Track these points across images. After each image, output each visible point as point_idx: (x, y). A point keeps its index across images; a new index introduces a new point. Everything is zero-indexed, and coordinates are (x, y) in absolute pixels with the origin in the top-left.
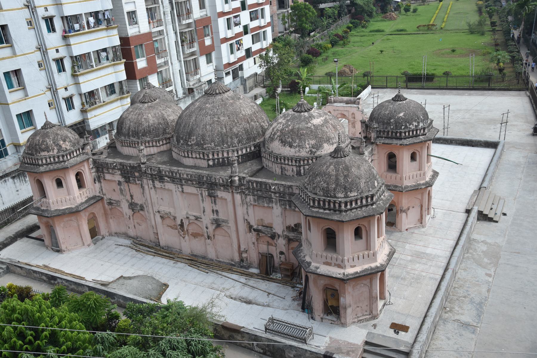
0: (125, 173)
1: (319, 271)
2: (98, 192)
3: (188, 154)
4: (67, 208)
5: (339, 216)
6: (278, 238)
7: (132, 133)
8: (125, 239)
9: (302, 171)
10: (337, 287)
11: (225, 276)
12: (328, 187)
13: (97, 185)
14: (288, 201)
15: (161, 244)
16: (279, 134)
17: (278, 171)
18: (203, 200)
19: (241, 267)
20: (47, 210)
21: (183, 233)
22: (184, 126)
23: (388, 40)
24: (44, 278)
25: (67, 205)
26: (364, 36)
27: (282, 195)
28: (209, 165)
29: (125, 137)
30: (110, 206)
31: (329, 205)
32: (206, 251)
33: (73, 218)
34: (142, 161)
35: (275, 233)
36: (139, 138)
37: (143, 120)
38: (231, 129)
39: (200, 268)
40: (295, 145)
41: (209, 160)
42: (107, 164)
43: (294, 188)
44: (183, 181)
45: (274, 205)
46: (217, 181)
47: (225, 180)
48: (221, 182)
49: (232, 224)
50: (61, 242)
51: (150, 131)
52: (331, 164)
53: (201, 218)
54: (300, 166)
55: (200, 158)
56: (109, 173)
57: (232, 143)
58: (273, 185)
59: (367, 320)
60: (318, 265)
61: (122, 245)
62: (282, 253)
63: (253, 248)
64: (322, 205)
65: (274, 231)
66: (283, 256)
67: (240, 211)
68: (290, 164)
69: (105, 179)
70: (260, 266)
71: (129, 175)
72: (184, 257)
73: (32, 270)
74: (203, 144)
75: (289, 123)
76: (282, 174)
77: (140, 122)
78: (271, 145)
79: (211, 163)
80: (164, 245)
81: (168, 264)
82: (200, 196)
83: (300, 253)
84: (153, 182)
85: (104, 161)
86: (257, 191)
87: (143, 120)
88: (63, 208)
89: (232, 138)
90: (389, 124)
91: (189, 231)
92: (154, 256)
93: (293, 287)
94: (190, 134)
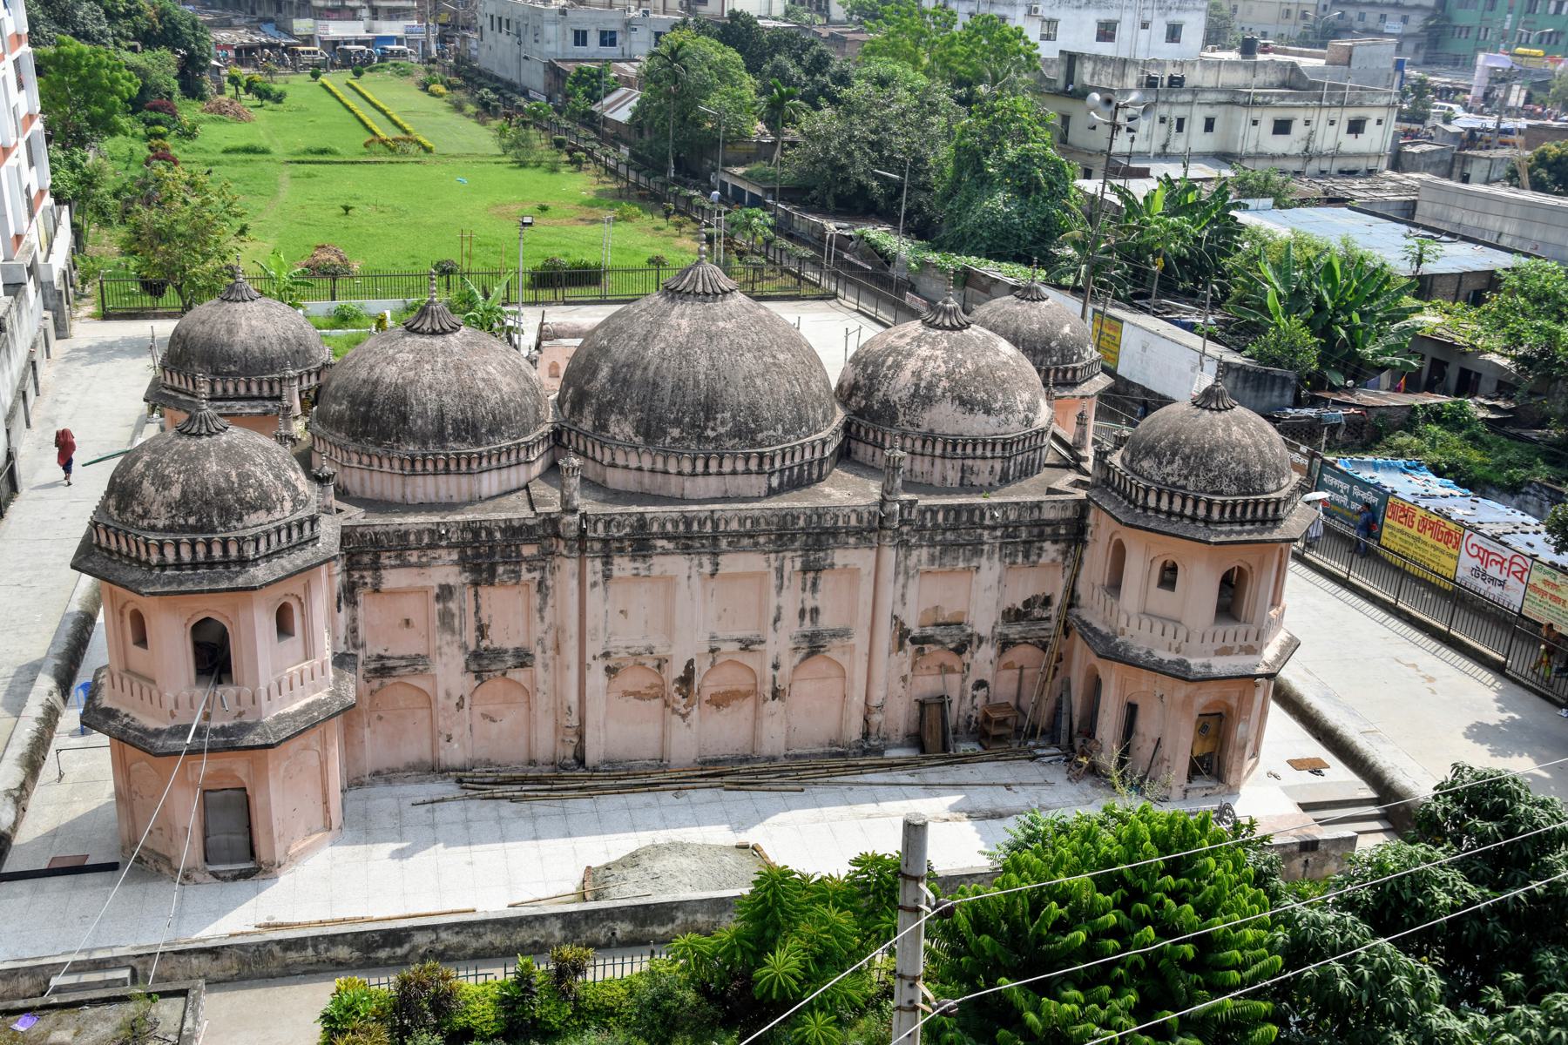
1: (1215, 671)
2: (342, 639)
3: (707, 466)
4: (309, 707)
7: (456, 428)
8: (422, 782)
10: (1233, 702)
11: (857, 784)
13: (343, 617)
14: (1025, 542)
15: (593, 755)
16: (944, 383)
17: (953, 477)
18: (780, 588)
19: (865, 753)
20: (244, 728)
21: (684, 701)
22: (677, 387)
23: (309, 176)
24: (342, 952)
25: (304, 695)
26: (218, 163)
27: (1009, 530)
29: (425, 444)
30: (376, 683)
32: (755, 737)
33: (313, 737)
35: (971, 635)
36: (478, 444)
40: (997, 405)
41: (771, 474)
42: (407, 533)
43: (1046, 507)
44: (724, 543)
45: (984, 561)
46: (840, 523)
47: (866, 515)
48: (853, 522)
49: (860, 640)
50: (276, 835)
52: (1227, 422)
53: (762, 642)
55: (748, 472)
56: (405, 564)
57: (815, 420)
58: (991, 507)
61: (443, 800)
62: (981, 684)
63: (900, 691)
65: (969, 630)
66: (982, 693)
68: (989, 454)
69: (377, 591)
70: (917, 740)
73: (279, 942)
74: (754, 432)
76: (961, 484)
77: (475, 391)
78: (927, 415)
79: (775, 482)
81: (663, 802)
83: (1126, 650)
84: (607, 562)
85: (391, 529)
86: (945, 531)
88: (296, 707)
90: (1047, 351)
92: (591, 796)
93: (1032, 759)
94: (710, 407)
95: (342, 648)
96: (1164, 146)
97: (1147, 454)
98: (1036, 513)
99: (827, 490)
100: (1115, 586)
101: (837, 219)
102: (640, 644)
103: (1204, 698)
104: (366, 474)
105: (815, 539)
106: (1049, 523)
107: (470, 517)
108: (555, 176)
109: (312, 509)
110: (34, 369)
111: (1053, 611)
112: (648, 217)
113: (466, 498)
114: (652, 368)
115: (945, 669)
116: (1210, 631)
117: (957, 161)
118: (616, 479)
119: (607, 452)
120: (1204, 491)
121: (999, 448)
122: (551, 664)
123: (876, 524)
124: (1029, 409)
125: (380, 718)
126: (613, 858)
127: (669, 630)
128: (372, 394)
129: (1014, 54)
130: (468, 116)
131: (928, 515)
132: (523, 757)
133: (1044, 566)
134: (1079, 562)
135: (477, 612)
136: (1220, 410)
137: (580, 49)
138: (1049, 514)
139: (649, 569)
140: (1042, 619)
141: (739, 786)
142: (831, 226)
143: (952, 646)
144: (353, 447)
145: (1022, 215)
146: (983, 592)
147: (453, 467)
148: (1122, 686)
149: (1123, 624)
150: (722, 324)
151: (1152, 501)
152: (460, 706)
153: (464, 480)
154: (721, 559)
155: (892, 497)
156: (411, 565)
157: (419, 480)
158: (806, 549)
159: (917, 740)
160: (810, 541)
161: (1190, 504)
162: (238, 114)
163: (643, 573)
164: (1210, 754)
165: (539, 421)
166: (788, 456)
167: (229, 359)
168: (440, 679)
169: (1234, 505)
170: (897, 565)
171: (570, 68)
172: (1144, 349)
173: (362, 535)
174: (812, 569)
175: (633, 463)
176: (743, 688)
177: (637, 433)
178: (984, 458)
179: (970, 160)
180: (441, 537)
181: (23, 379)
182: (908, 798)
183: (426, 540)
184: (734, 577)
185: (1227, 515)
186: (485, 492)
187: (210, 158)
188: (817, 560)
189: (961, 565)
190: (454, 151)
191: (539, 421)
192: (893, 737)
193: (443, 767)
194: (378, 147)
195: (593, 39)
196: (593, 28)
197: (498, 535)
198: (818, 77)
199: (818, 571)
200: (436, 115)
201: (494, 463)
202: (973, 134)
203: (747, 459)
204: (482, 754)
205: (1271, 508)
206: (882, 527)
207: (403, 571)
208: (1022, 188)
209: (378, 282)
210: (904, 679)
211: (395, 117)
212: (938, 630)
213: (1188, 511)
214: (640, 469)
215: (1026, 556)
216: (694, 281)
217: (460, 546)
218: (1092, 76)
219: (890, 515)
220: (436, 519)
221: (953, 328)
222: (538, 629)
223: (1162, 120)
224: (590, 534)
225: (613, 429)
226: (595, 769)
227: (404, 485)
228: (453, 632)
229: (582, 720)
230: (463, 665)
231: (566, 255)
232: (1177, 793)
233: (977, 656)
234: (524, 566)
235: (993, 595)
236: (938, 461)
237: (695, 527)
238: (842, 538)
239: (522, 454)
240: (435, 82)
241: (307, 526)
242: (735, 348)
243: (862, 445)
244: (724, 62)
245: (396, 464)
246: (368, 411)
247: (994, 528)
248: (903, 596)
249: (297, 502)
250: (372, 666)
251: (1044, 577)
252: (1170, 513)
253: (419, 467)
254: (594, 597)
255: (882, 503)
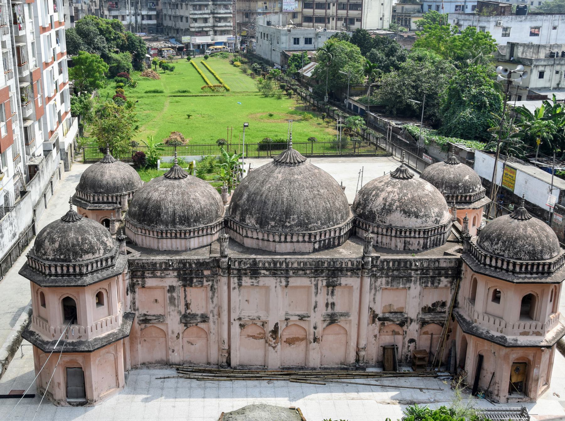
0: (185, 274)
1: (519, 343)
3: (286, 238)
5: (550, 278)
6: (410, 324)
9: (428, 244)
10: (531, 358)
11: (351, 383)
12: (534, 250)
13: (129, 297)
14: (431, 277)
15: (234, 363)
16: (397, 204)
17: (400, 246)
18: (317, 293)
19: (357, 369)
21: (274, 341)
22: (274, 204)
23: (177, 102)
26: (142, 97)
28: (314, 248)
29: (167, 225)
31: (538, 268)
34: (226, 253)
35: (407, 318)
36: (189, 226)
37: (192, 201)
38: (334, 203)
39: (308, 382)
40: (421, 214)
41: (315, 243)
42: (156, 263)
44: (291, 273)
45: (412, 285)
46: (344, 266)
47: (355, 263)
48: (350, 265)
49: (354, 317)
51: (203, 215)
52: (525, 226)
53: (309, 317)
54: (427, 238)
55: (304, 241)
56: (155, 277)
57: (337, 219)
58: (415, 260)
59: (545, 390)
60: (514, 337)
62: (412, 341)
64: (529, 270)
65: (406, 316)
66: (412, 345)
67: (367, 298)
68: (417, 236)
69: (143, 287)
70: (381, 364)
71: (193, 275)
72: (276, 373)
74: (307, 224)
75: (405, 191)
76: (404, 249)
77: (189, 204)
78: (388, 218)
79: (317, 246)
80: (238, 363)
81: (262, 385)
82: (314, 287)
83: (477, 330)
84: (240, 279)
85: (149, 261)
86: (393, 270)
87: (192, 201)
89: (336, 214)
90: (457, 188)
91: (282, 337)
92: (231, 380)
93: (435, 377)
94: (288, 213)
95: (129, 310)
96: (558, 84)
97: (487, 239)
98: (437, 264)
99: (341, 250)
100: (473, 300)
101: (397, 120)
102: (254, 315)
103: (515, 355)
104: (144, 237)
105: (332, 273)
106: (443, 269)
107: (182, 258)
108: (280, 101)
109: (112, 253)
110: (52, 184)
111: (447, 309)
112: (316, 119)
113: (184, 249)
114: (264, 195)
115: (395, 333)
116: (517, 324)
117: (450, 95)
118: (248, 242)
119: (244, 231)
120: (512, 258)
121: (422, 233)
122: (216, 322)
123: (360, 266)
124: (438, 216)
125: (145, 340)
126: (235, 409)
127: (267, 310)
128: (147, 204)
129: (483, 45)
130: (248, 75)
131: (385, 263)
132: (205, 361)
133: (441, 288)
134: (458, 287)
135: (185, 298)
136: (522, 220)
137: (296, 46)
138: (443, 265)
139: (258, 282)
140: (441, 312)
141: (297, 380)
142: (393, 123)
143: (398, 322)
144: (139, 226)
145: (478, 118)
146: (413, 299)
147: (178, 235)
148: (476, 346)
149: (476, 317)
150: (296, 176)
151: (488, 262)
152: (178, 337)
153: (183, 241)
154: (290, 279)
155: (368, 255)
156: (157, 277)
157: (165, 240)
158: (328, 277)
159: (381, 364)
160: (330, 273)
161: (505, 263)
162: (154, 77)
163: (255, 284)
164: (521, 382)
165: (217, 216)
166: (323, 235)
167: (101, 187)
168: (169, 325)
169: (527, 265)
170: (371, 285)
171: (290, 54)
172: (526, 182)
173: (137, 263)
174: (332, 286)
175: (255, 236)
176: (301, 337)
177: (257, 223)
178: (415, 238)
179: (455, 94)
180: (170, 266)
181: (46, 189)
182: (373, 391)
183: (164, 267)
184: (296, 287)
185: (523, 269)
186: (192, 246)
187: (139, 95)
188: (333, 282)
189: (401, 286)
190: (238, 90)
191: (217, 216)
192: (371, 363)
193: (171, 363)
194: (207, 89)
195: (302, 41)
196: (302, 37)
197: (194, 266)
198: (391, 58)
199: (334, 286)
200: (234, 75)
201: (196, 234)
202: (457, 83)
203: (304, 236)
204: (187, 358)
205: (546, 267)
206: (363, 268)
207: (154, 279)
208: (478, 106)
209: (194, 148)
210: (375, 336)
211: (217, 76)
212: (391, 315)
213: (505, 267)
214: (258, 239)
215: (433, 283)
216: (286, 158)
217: (178, 270)
218: (523, 53)
219: (367, 263)
220: (168, 258)
221: (404, 178)
222: (211, 306)
223: (557, 72)
224: (232, 267)
225: (247, 221)
226: (235, 368)
227: (158, 243)
228: (175, 306)
229: (229, 346)
230: (179, 320)
231: (276, 136)
232: (503, 399)
233: (410, 328)
234: (205, 279)
235: (417, 300)
236: (393, 239)
237: (278, 265)
238: (345, 272)
239: (209, 231)
240: (236, 61)
241: (109, 260)
242: (301, 187)
243: (360, 230)
244: (352, 52)
245: (155, 234)
246: (145, 211)
247: (417, 270)
248: (374, 299)
249: (105, 249)
250: (141, 318)
251: (441, 293)
252: (496, 267)
253: (164, 235)
254: (235, 294)
255: (363, 258)
